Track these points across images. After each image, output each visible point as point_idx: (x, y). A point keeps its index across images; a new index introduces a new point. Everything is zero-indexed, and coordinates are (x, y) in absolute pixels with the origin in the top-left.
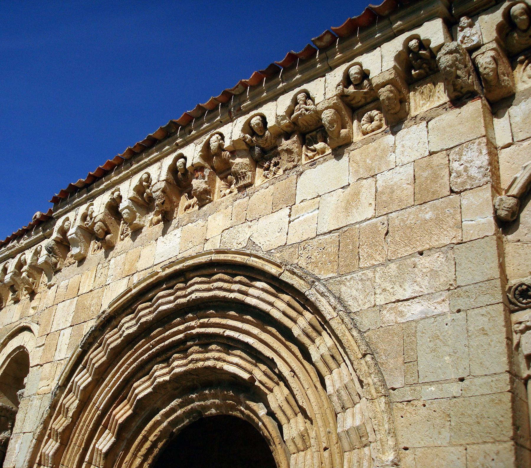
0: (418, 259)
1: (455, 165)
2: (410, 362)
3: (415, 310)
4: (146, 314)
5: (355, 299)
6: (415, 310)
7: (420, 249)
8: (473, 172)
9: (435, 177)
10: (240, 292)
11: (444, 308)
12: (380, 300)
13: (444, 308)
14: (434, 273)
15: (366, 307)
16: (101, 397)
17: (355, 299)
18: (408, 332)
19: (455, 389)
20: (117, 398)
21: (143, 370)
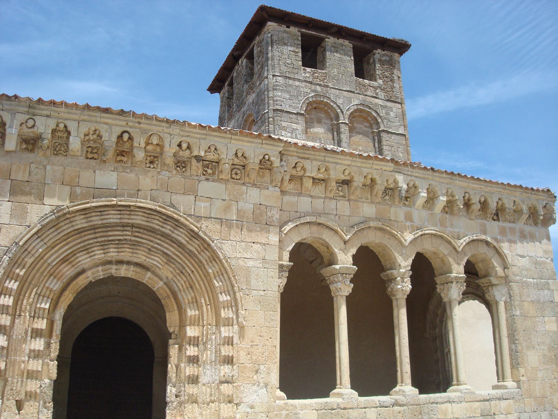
0: (253, 244)
1: (268, 213)
2: (248, 282)
3: (250, 263)
4: (96, 220)
5: (228, 252)
6: (250, 263)
7: (254, 241)
8: (274, 219)
9: (261, 215)
10: (170, 230)
11: (260, 265)
12: (238, 255)
13: (260, 265)
14: (258, 252)
15: (233, 256)
16: (53, 258)
17: (228, 252)
18: (248, 270)
19: (262, 293)
20: (64, 261)
21: (86, 249)
